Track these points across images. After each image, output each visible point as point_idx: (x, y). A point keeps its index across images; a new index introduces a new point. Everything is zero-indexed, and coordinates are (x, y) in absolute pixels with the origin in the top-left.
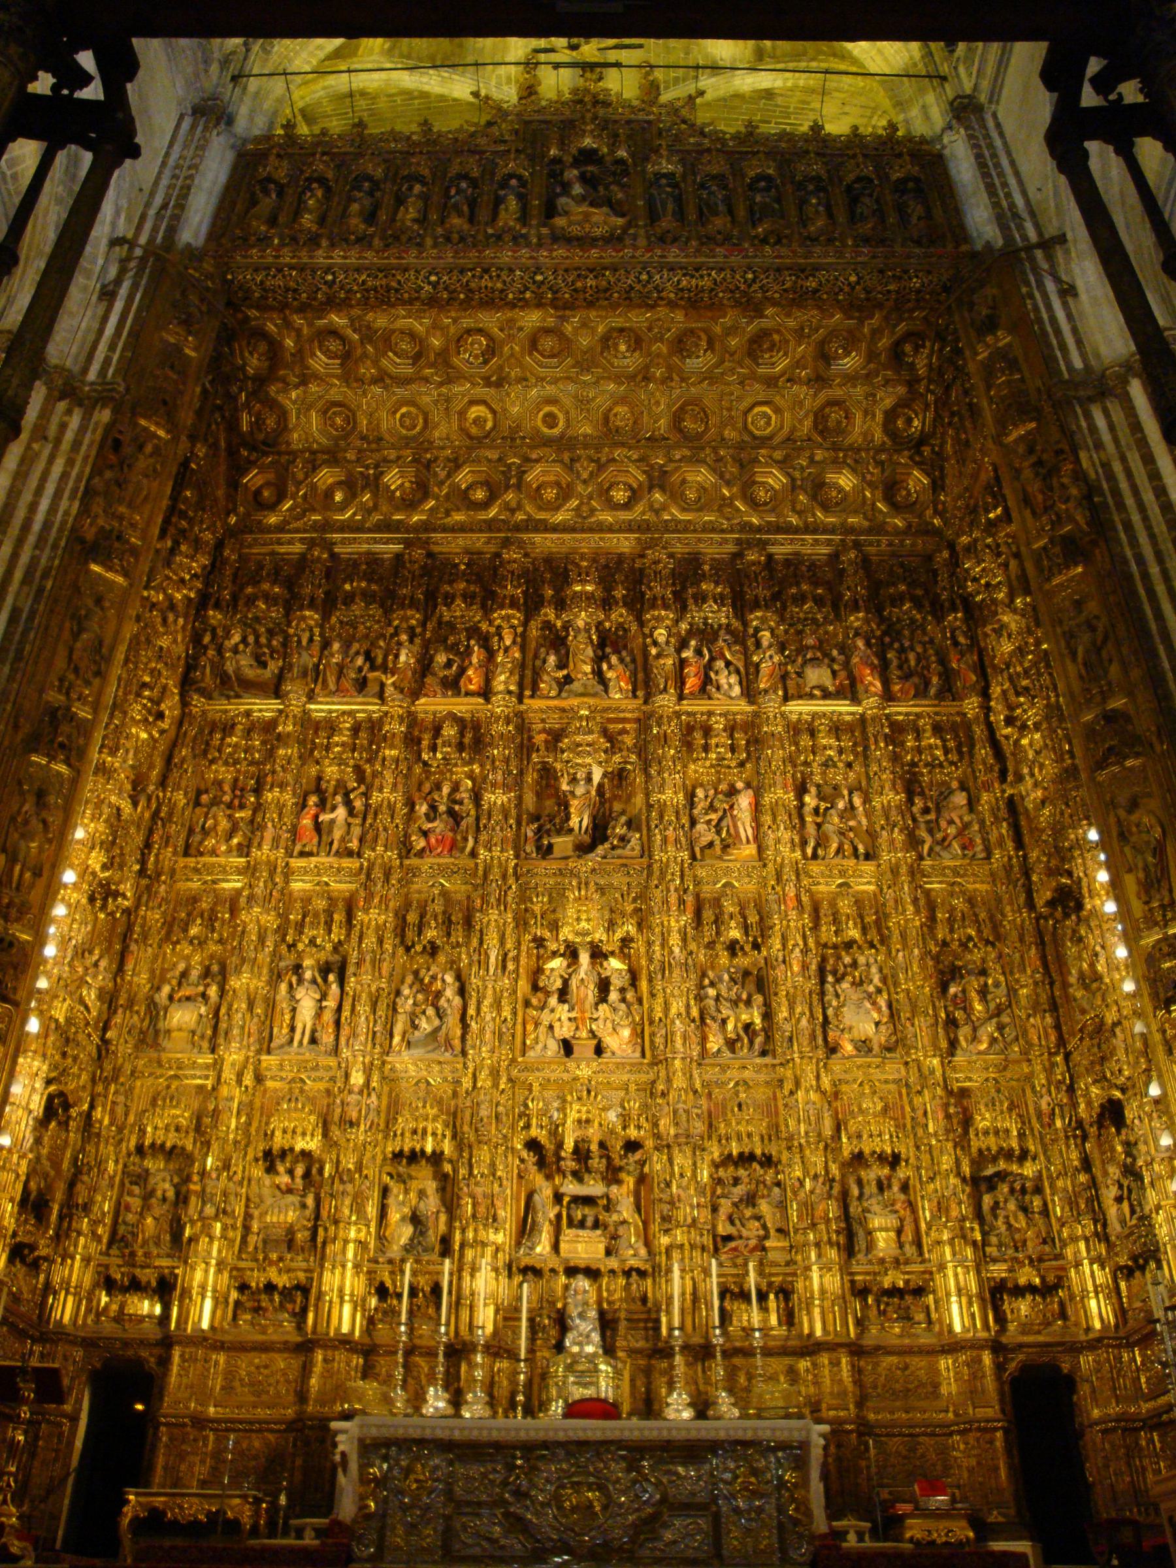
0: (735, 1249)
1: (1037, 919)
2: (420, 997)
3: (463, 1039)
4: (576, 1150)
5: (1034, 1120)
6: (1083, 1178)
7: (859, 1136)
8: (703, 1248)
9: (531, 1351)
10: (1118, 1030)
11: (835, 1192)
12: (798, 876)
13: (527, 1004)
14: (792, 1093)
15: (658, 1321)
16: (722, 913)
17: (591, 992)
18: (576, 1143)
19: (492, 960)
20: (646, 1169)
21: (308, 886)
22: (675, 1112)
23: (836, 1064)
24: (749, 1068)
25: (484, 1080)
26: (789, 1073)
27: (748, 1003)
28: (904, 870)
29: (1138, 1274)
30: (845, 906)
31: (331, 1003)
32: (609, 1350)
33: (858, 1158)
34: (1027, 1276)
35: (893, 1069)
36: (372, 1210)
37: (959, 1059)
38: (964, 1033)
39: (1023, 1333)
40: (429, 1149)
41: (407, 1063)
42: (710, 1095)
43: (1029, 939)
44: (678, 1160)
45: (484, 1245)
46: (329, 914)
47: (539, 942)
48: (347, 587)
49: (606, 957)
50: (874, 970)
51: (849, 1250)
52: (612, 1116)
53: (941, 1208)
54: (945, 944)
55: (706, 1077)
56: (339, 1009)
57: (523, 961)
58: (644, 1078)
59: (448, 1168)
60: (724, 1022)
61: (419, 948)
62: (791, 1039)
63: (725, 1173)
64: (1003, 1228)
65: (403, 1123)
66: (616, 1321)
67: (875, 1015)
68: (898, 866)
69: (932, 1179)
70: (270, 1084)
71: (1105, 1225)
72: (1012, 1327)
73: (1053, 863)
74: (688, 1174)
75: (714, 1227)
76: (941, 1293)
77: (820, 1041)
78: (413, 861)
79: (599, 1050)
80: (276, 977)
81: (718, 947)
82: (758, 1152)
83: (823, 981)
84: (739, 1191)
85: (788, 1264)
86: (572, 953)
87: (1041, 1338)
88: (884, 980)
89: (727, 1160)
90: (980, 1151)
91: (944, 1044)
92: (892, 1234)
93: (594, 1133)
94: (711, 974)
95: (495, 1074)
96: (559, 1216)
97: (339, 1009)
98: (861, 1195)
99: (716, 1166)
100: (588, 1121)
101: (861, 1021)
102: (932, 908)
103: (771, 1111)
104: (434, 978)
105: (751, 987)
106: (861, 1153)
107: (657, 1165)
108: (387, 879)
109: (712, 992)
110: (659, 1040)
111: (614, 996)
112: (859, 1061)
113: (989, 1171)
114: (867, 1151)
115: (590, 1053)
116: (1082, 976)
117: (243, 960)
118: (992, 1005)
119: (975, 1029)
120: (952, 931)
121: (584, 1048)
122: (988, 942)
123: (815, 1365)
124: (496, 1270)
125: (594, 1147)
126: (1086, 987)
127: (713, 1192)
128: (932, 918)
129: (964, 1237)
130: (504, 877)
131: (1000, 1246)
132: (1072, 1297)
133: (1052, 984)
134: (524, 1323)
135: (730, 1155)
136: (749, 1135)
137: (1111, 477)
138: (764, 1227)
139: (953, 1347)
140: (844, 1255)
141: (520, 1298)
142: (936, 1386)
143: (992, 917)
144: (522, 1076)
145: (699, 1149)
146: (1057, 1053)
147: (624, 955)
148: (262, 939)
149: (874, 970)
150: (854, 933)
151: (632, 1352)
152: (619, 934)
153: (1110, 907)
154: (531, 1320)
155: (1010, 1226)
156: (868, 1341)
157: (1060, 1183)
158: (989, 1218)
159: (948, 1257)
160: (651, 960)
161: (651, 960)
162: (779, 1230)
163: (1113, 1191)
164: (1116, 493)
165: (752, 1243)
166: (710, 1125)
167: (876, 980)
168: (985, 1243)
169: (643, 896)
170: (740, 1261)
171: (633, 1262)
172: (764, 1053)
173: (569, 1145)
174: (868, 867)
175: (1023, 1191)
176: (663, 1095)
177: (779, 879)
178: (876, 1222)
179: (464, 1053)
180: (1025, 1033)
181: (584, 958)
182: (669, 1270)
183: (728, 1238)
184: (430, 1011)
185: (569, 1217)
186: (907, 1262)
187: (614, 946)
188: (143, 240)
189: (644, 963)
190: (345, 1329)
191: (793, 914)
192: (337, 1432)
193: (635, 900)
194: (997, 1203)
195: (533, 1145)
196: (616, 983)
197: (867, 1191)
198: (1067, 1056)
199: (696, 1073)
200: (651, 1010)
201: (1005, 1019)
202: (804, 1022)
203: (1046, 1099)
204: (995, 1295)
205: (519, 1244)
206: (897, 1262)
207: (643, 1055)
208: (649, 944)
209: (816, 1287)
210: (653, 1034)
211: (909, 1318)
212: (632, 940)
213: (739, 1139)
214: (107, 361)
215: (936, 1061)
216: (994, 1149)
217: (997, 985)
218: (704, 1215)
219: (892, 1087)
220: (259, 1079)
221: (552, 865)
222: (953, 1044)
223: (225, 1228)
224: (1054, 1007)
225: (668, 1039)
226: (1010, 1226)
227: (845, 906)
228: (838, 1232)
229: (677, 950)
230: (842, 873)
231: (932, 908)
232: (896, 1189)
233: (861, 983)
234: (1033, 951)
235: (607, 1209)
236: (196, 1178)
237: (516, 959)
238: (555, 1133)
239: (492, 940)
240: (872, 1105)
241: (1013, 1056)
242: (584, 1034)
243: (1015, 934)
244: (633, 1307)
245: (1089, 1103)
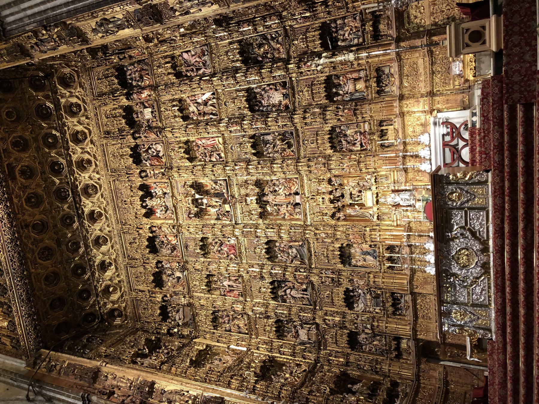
40: (339, 253)
59: (344, 245)
75: (357, 151)
79: (297, 193)
90: (321, 47)
118: (264, 41)
137: (34, 15)
164: (39, 13)
165: (362, 137)
171: (373, 180)
183: (361, 145)
188: (27, 386)
214: (74, 398)
236: (357, 331)
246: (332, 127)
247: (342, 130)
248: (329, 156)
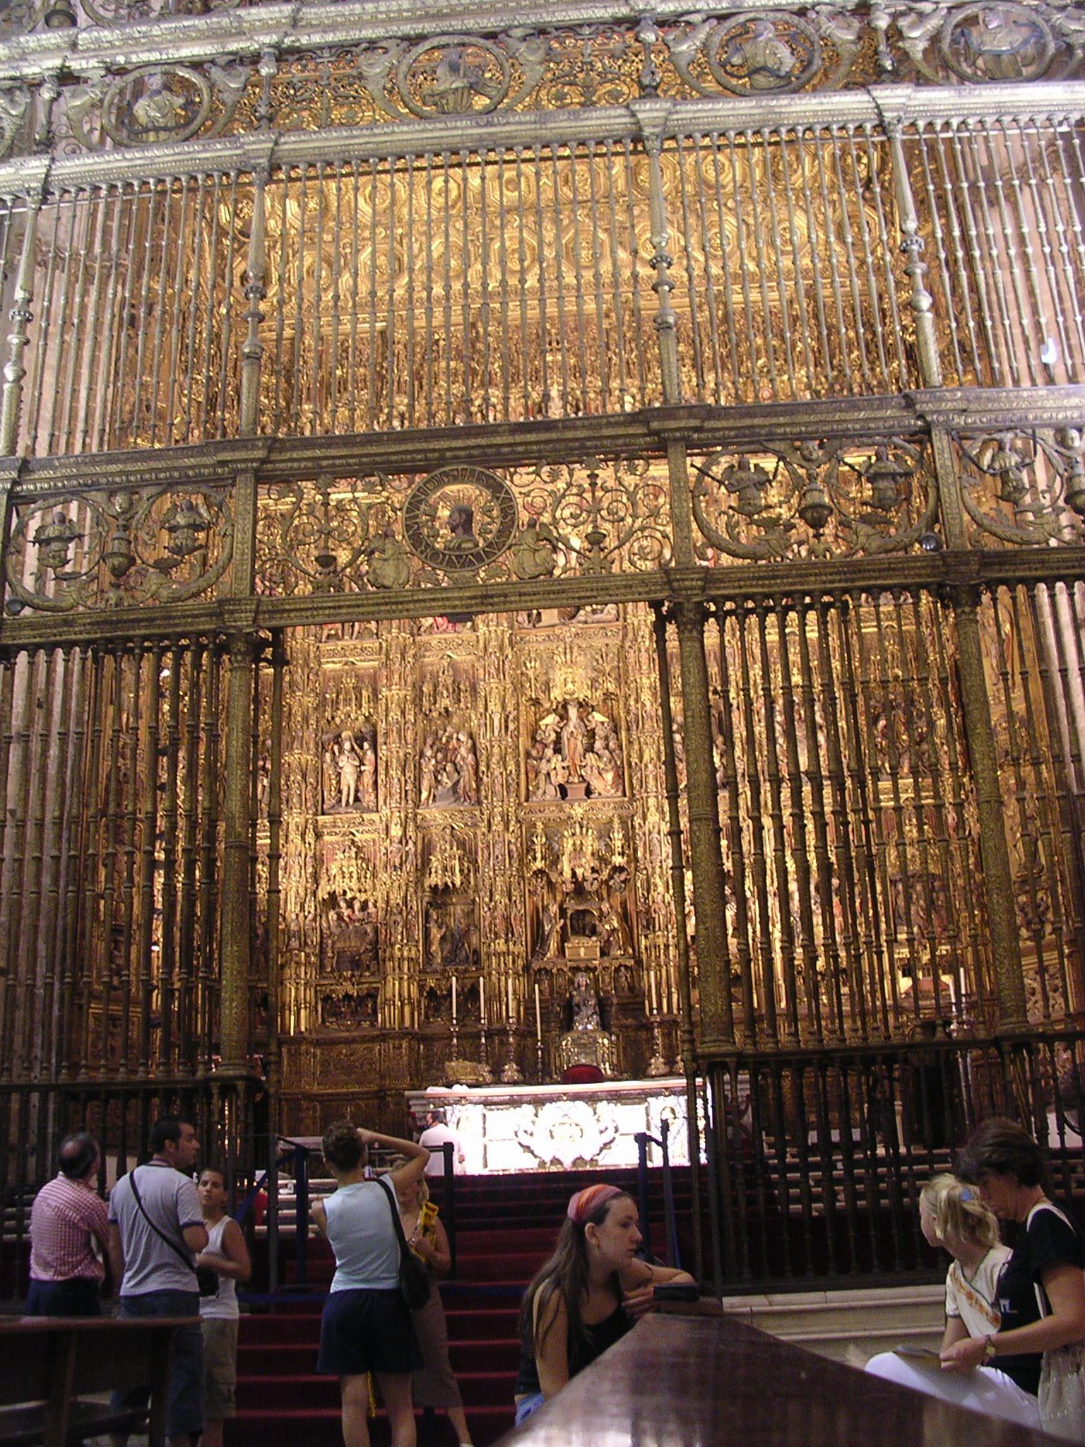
2: (440, 756)
17: (580, 743)
19: (496, 723)
21: (338, 666)
25: (498, 826)
31: (368, 768)
32: (604, 1026)
36: (418, 934)
41: (436, 815)
46: (358, 690)
48: (339, 372)
56: (376, 771)
61: (435, 714)
65: (435, 863)
70: (326, 838)
78: (425, 638)
79: (588, 792)
80: (322, 748)
96: (563, 928)
97: (376, 771)
104: (450, 737)
108: (403, 658)
111: (598, 745)
117: (293, 739)
121: (577, 791)
130: (501, 648)
148: (306, 719)
160: (628, 713)
161: (628, 713)
179: (479, 803)
181: (573, 712)
184: (449, 767)
190: (407, 1023)
192: (409, 1099)
196: (600, 732)
200: (629, 756)
220: (318, 836)
221: (542, 634)
223: (307, 956)
229: (648, 704)
237: (517, 719)
239: (494, 706)
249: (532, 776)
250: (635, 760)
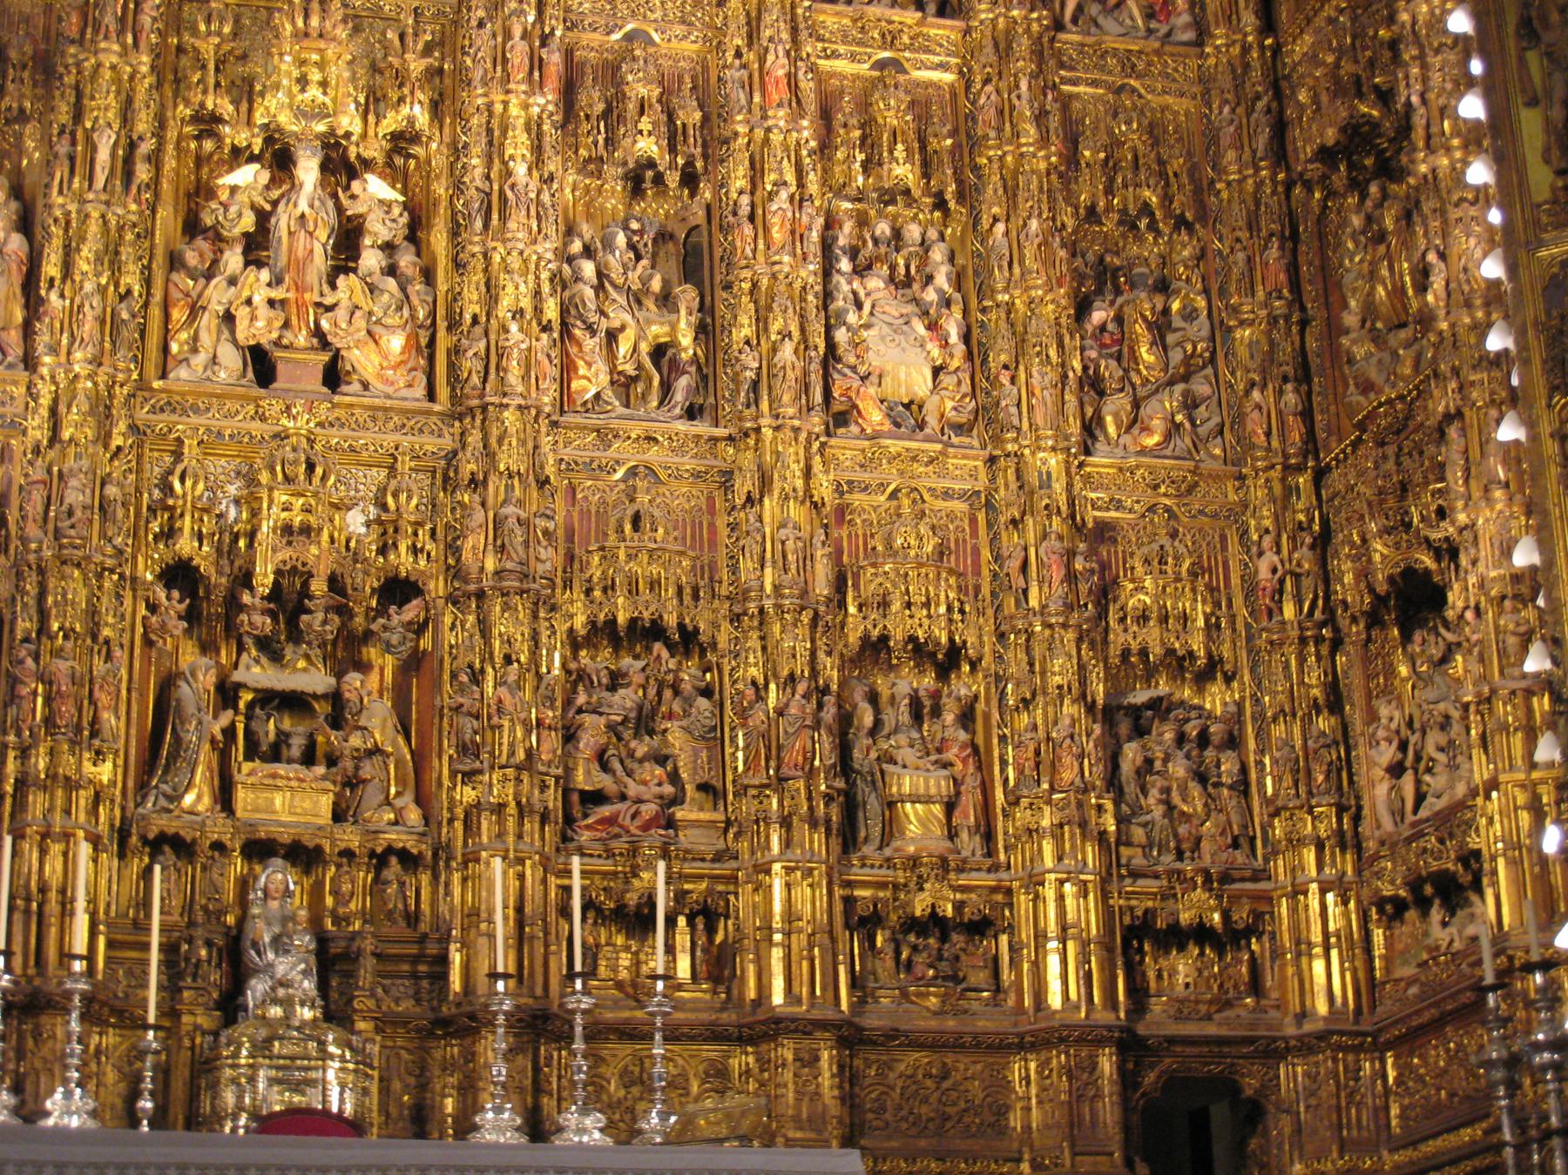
0: (611, 821)
1: (1289, 186)
3: (28, 330)
4: (276, 593)
5: (1238, 601)
6: (1323, 723)
7: (884, 604)
8: (544, 818)
9: (170, 1012)
10: (1453, 432)
11: (829, 713)
12: (794, 31)
13: (175, 262)
14: (749, 499)
15: (443, 960)
16: (621, 97)
17: (318, 249)
18: (278, 573)
19: (103, 155)
20: (426, 643)
22: (498, 523)
23: (846, 447)
24: (663, 442)
26: (747, 459)
27: (666, 300)
28: (1023, 45)
29: (1411, 914)
30: (892, 113)
33: (875, 649)
34: (1195, 906)
35: (965, 466)
37: (1101, 461)
38: (1115, 407)
39: (1179, 1017)
42: (572, 490)
43: (1268, 225)
44: (502, 626)
45: (71, 785)
47: (208, 123)
49: (353, 174)
50: (938, 254)
51: (848, 837)
52: (355, 521)
53: (1042, 763)
54: (1092, 214)
55: (567, 453)
57: (170, 163)
58: (430, 444)
60: (612, 336)
62: (755, 385)
63: (597, 661)
64: (1158, 812)
66: (351, 958)
67: (935, 352)
68: (1009, 34)
69: (1026, 703)
71: (1357, 819)
72: (1157, 1006)
73: (1347, 68)
74: (516, 659)
75: (569, 771)
76: (1026, 933)
77: (818, 397)
79: (334, 377)
81: (611, 171)
82: (671, 620)
83: (827, 271)
84: (625, 700)
85: (718, 857)
86: (280, 160)
87: (1211, 1030)
88: (958, 281)
89: (604, 632)
90: (1126, 653)
91: (1074, 428)
92: (937, 809)
93: (318, 556)
94: (586, 230)
95: (102, 412)
96: (229, 732)
98: (878, 723)
99: (575, 643)
100: (306, 530)
101: (901, 358)
102: (1072, 143)
103: (698, 534)
105: (673, 267)
106: (884, 638)
107: (453, 633)
109: (588, 268)
110: (470, 364)
111: (371, 260)
112: (894, 446)
113: (1140, 697)
114: (898, 636)
115: (315, 384)
116: (1370, 310)
118: (1176, 356)
119: (1136, 405)
120: (1109, 191)
121: (300, 369)
122: (1181, 223)
123: (763, 1063)
124: (95, 840)
125: (318, 586)
126: (1377, 339)
127: (568, 702)
128: (1071, 158)
129: (1083, 824)
131: (1147, 847)
132: (1277, 954)
133: (1304, 324)
134: (155, 956)
135: (612, 622)
136: (654, 584)
138: (674, 778)
139: (1044, 1037)
140: (836, 847)
141: (146, 904)
142: (1002, 1111)
143: (1193, 170)
144: (161, 422)
145: (542, 604)
146: (1300, 469)
147: (393, 174)
149: (938, 254)
150: (903, 171)
151: (385, 1023)
152: (392, 122)
153: (1479, 173)
154: (169, 949)
155: (1170, 807)
156: (872, 1021)
157: (1278, 731)
158: (1131, 789)
159: (1049, 862)
160: (458, 187)
161: (458, 187)
162: (704, 787)
163: (1387, 754)
165: (649, 810)
166: (570, 557)
167: (941, 280)
168: (1123, 839)
169: (448, 42)
170: (620, 845)
171: (394, 837)
172: (692, 413)
173: (264, 578)
174: (944, 31)
175: (1204, 739)
176: (475, 483)
177: (752, 37)
178: (906, 783)
179: (30, 362)
180: (1239, 418)
181: (308, 170)
182: (471, 858)
183: (595, 798)
185: (248, 732)
186: (960, 870)
187: (374, 150)
189: (441, 189)
191: (780, 117)
193: (428, 50)
194: (1149, 762)
195: (180, 575)
196: (379, 229)
197: (889, 718)
198: (1320, 476)
199: (546, 441)
200: (455, 297)
201: (1201, 387)
202: (787, 352)
203: (1270, 558)
204: (1134, 940)
205: (142, 787)
206: (944, 862)
207: (431, 395)
208: (457, 151)
209: (777, 907)
210: (456, 352)
211: (956, 979)
212: (415, 138)
213: (633, 590)
215: (1054, 462)
216: (1156, 652)
217: (1189, 314)
218: (551, 743)
219: (960, 506)
222: (1091, 429)
224: (1304, 375)
225: (493, 361)
226: (1170, 807)
227: (892, 113)
228: (829, 799)
230: (890, 39)
231: (1072, 143)
232: (949, 718)
233: (908, 282)
234: (1273, 252)
235: (336, 721)
237: (155, 159)
238: (234, 547)
239: (104, 107)
240: (919, 541)
241: (1208, 465)
242: (302, 339)
243: (1238, 215)
244: (387, 930)
245: (1364, 574)
246: (714, 645)
247: (689, 702)
248: (553, 608)
249: (178, 315)
250: (472, 306)
